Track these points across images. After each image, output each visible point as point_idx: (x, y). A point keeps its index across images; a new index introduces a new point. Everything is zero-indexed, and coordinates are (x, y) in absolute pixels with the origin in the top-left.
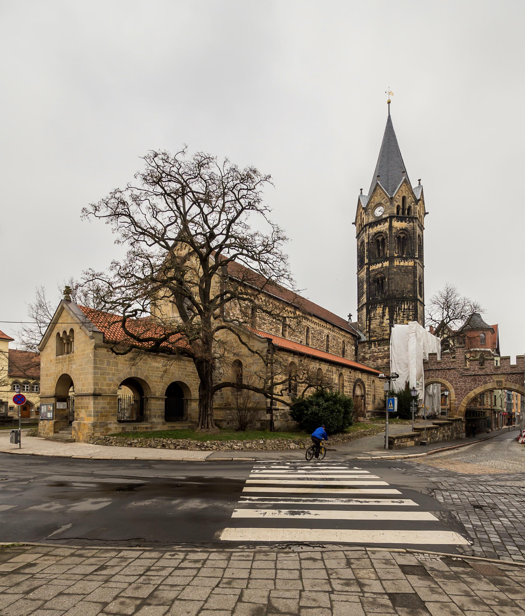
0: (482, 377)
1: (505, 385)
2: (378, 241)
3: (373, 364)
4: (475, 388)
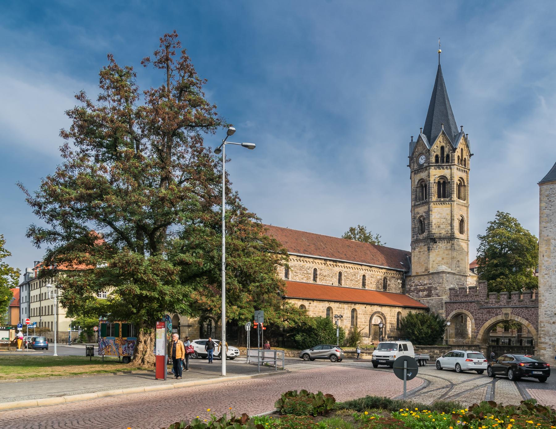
0: (495, 309)
1: (511, 317)
2: (422, 185)
3: (416, 296)
4: (489, 319)
